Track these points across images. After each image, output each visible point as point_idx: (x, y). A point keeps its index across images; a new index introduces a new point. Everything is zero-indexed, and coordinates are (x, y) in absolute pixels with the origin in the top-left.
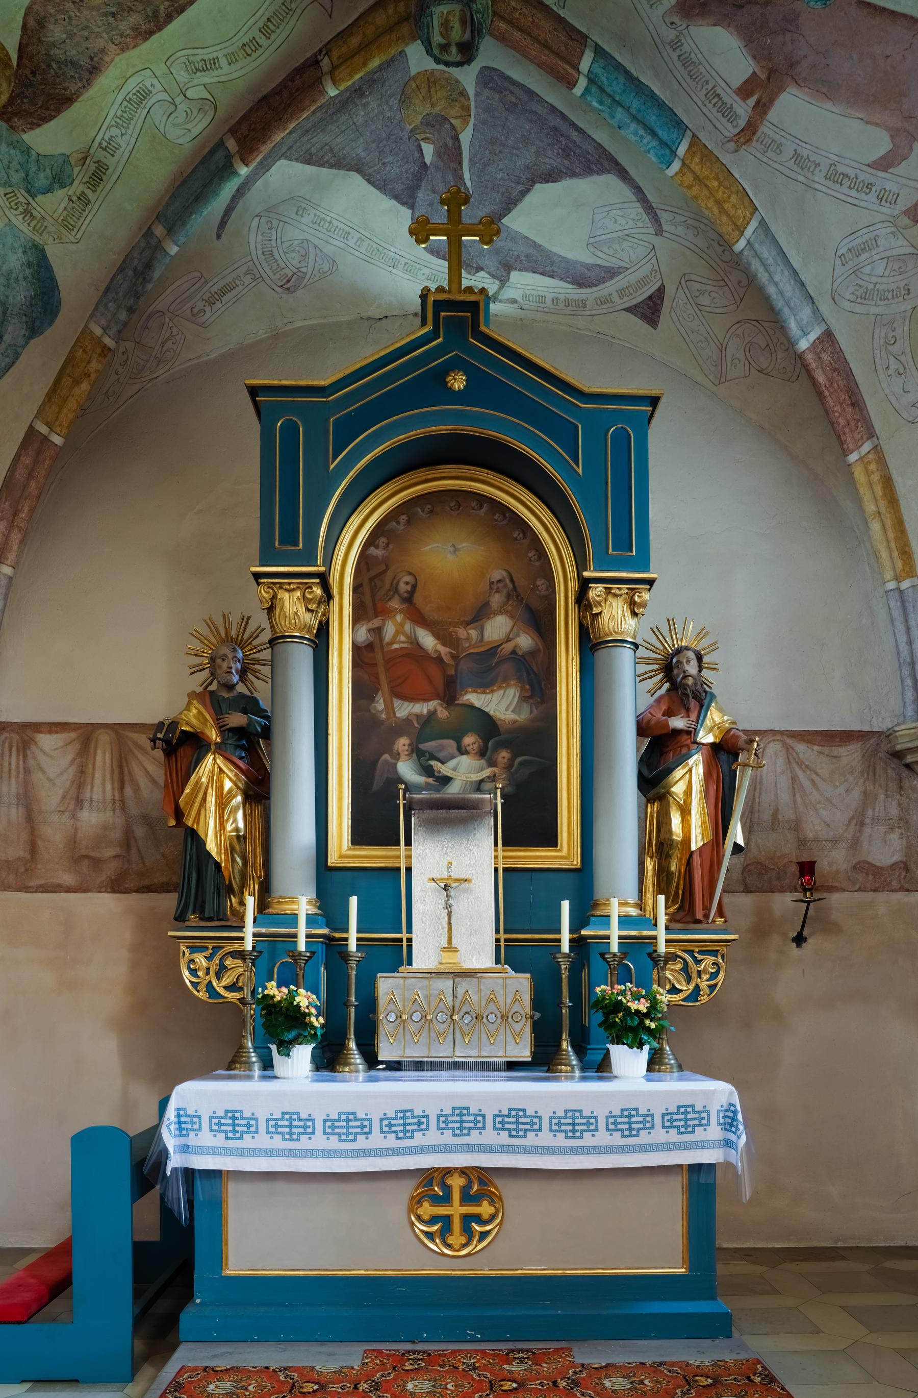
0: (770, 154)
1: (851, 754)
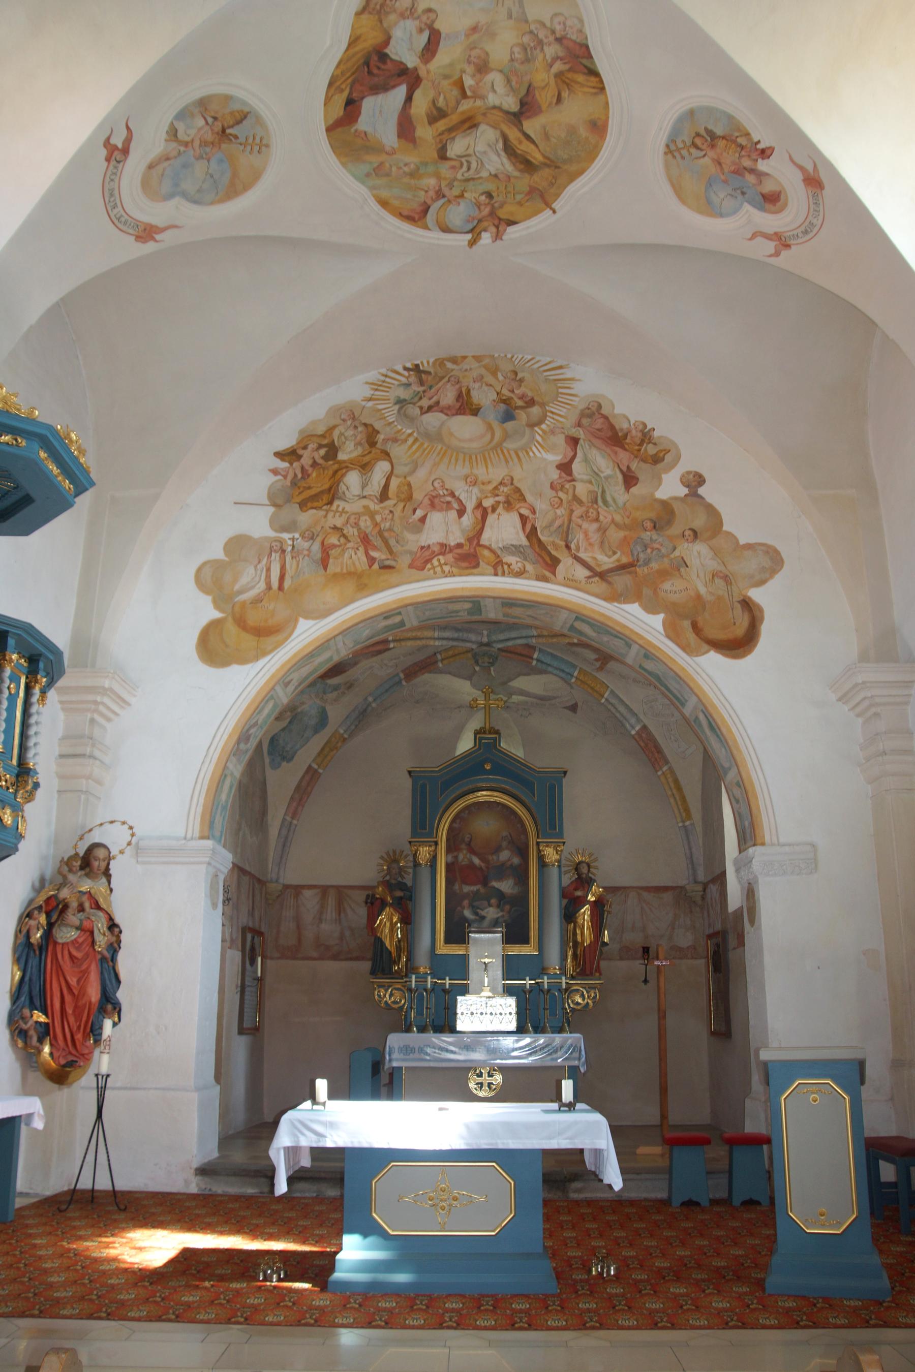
1: (668, 897)
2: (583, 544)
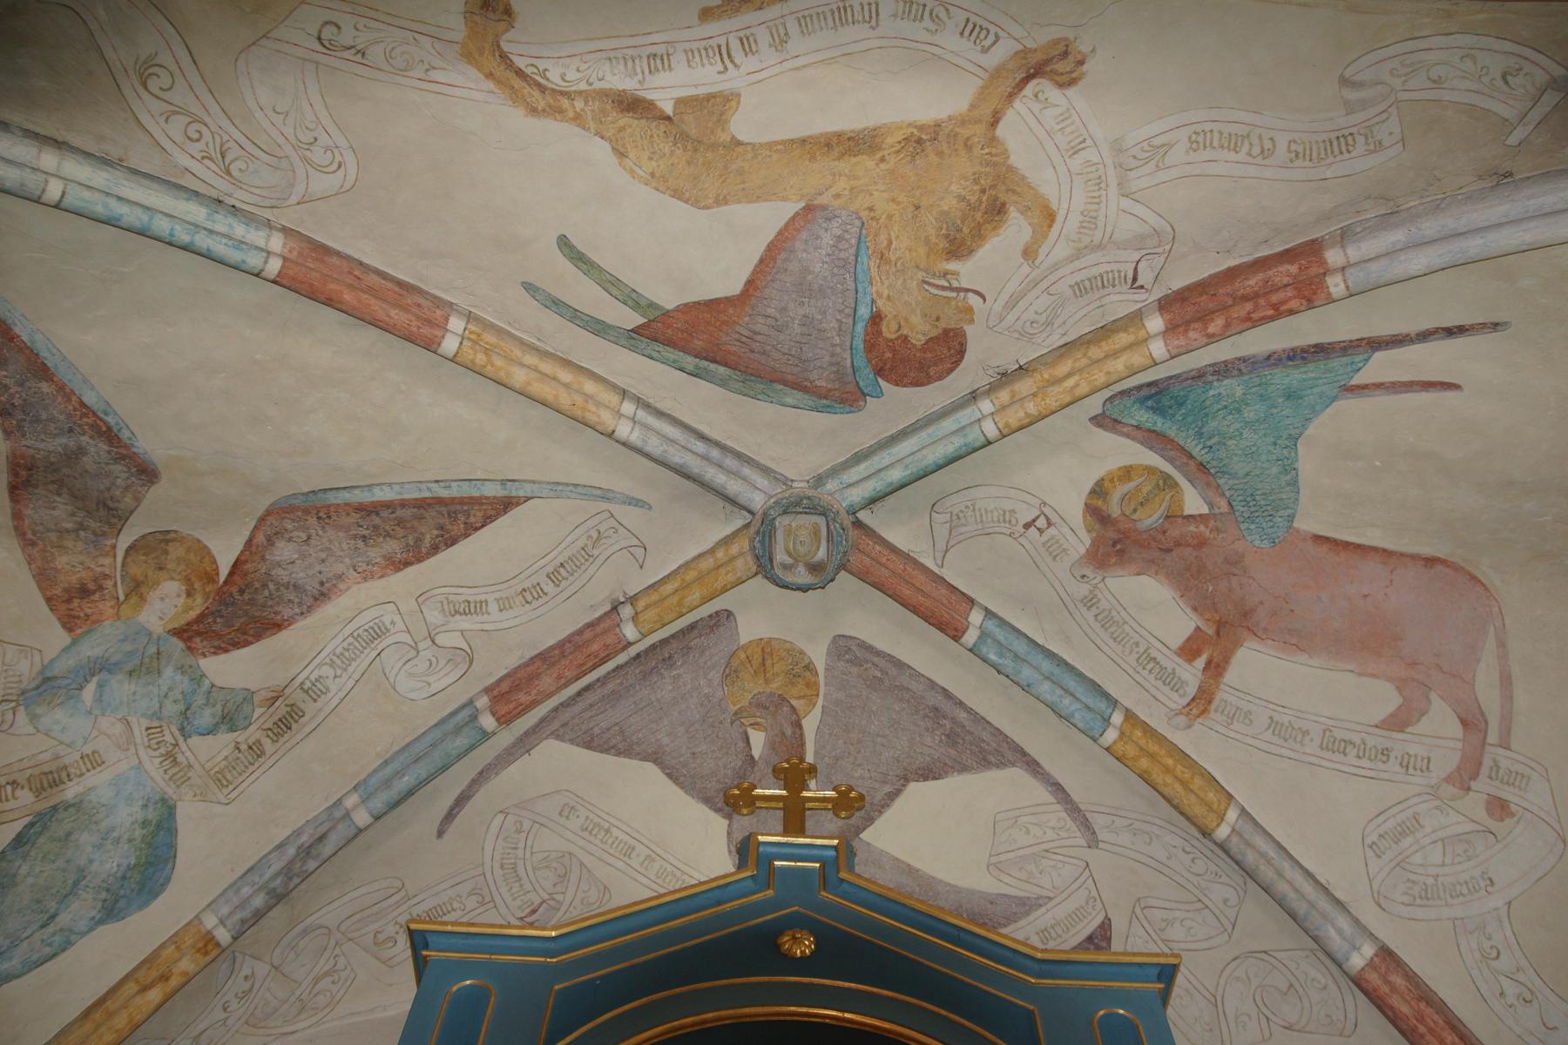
0: (1236, 726)
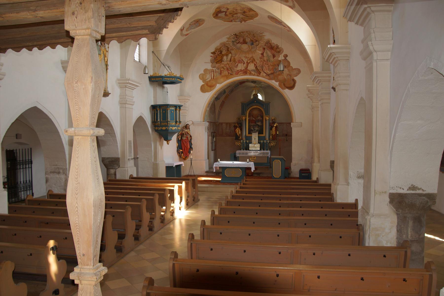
2: (265, 69)
